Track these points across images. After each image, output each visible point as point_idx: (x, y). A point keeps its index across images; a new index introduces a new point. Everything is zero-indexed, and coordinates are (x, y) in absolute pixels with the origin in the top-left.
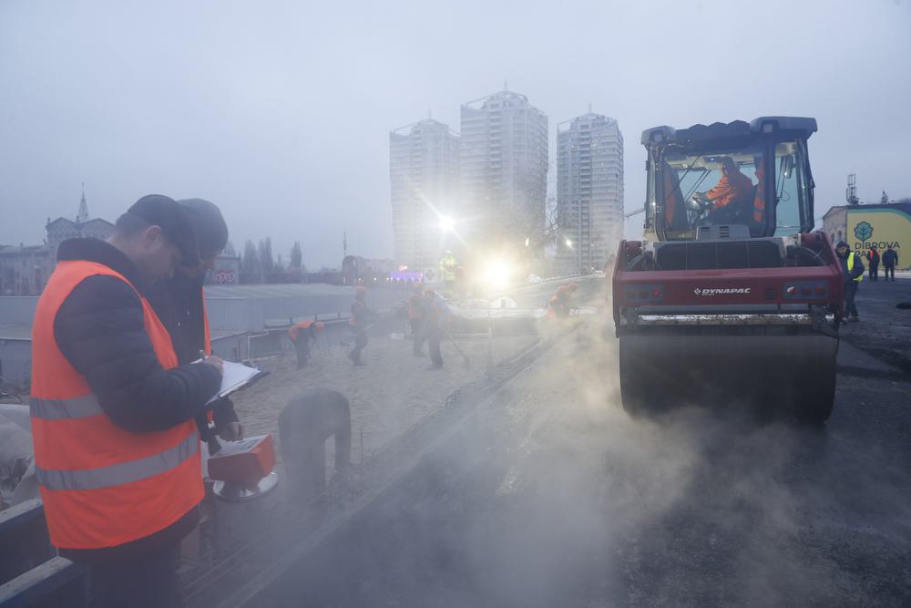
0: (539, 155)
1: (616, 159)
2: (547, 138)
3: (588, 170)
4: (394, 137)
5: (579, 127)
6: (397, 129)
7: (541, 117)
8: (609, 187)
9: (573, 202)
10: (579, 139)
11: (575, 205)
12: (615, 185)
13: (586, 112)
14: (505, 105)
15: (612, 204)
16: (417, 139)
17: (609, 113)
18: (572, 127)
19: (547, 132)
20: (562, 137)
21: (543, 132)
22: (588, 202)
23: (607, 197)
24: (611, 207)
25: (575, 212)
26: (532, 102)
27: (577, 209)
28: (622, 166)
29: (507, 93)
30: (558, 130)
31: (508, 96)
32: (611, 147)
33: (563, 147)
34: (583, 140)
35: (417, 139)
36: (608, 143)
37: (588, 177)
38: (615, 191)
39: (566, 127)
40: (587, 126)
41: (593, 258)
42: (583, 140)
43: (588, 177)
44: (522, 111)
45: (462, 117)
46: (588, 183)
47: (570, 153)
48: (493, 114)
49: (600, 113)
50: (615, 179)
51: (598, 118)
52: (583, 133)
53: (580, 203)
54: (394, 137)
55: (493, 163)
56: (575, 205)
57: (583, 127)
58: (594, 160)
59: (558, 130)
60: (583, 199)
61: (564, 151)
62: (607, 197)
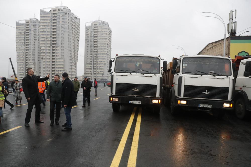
0: (74, 33)
1: (108, 38)
2: (79, 27)
3: (97, 42)
4: (18, 24)
5: (94, 25)
6: (18, 21)
7: (76, 18)
8: (104, 49)
9: (90, 54)
10: (93, 29)
11: (91, 55)
12: (107, 48)
13: (98, 19)
14: (59, 10)
15: (106, 55)
16: (27, 25)
17: (106, 21)
18: (91, 25)
19: (79, 25)
20: (87, 28)
21: (77, 24)
22: (96, 54)
23: (104, 53)
24: (105, 56)
25: (91, 58)
26: (72, 12)
27: (92, 57)
28: (111, 41)
29: (62, 6)
30: (86, 25)
31: (62, 8)
32: (107, 33)
33: (87, 32)
34: (95, 30)
35: (27, 25)
36: (104, 31)
37: (96, 44)
38: (107, 50)
39: (89, 24)
40: (97, 24)
41: (98, 76)
42: (95, 30)
43: (96, 44)
44: (66, 13)
45: (41, 14)
46: (96, 47)
47: (90, 35)
48: (54, 14)
49: (103, 20)
50: (107, 45)
51: (102, 22)
52: (95, 27)
53: (93, 54)
54: (18, 24)
55: (53, 35)
56: (91, 55)
57: (95, 25)
58: (99, 38)
59: (86, 25)
60: (94, 53)
61: (88, 34)
62: (104, 53)
